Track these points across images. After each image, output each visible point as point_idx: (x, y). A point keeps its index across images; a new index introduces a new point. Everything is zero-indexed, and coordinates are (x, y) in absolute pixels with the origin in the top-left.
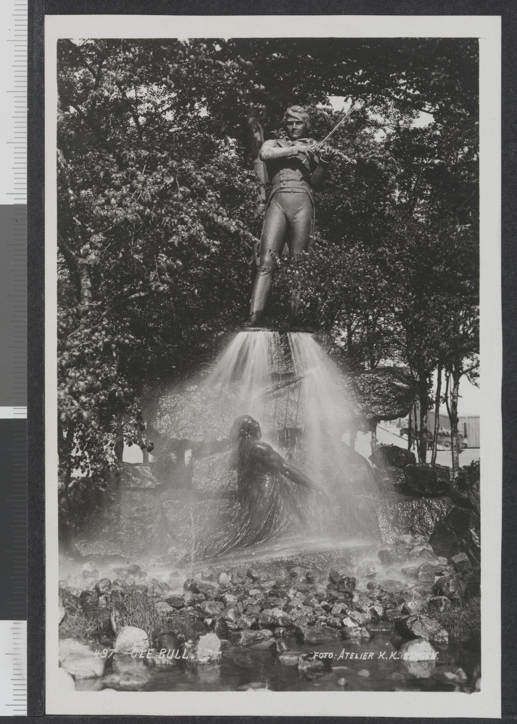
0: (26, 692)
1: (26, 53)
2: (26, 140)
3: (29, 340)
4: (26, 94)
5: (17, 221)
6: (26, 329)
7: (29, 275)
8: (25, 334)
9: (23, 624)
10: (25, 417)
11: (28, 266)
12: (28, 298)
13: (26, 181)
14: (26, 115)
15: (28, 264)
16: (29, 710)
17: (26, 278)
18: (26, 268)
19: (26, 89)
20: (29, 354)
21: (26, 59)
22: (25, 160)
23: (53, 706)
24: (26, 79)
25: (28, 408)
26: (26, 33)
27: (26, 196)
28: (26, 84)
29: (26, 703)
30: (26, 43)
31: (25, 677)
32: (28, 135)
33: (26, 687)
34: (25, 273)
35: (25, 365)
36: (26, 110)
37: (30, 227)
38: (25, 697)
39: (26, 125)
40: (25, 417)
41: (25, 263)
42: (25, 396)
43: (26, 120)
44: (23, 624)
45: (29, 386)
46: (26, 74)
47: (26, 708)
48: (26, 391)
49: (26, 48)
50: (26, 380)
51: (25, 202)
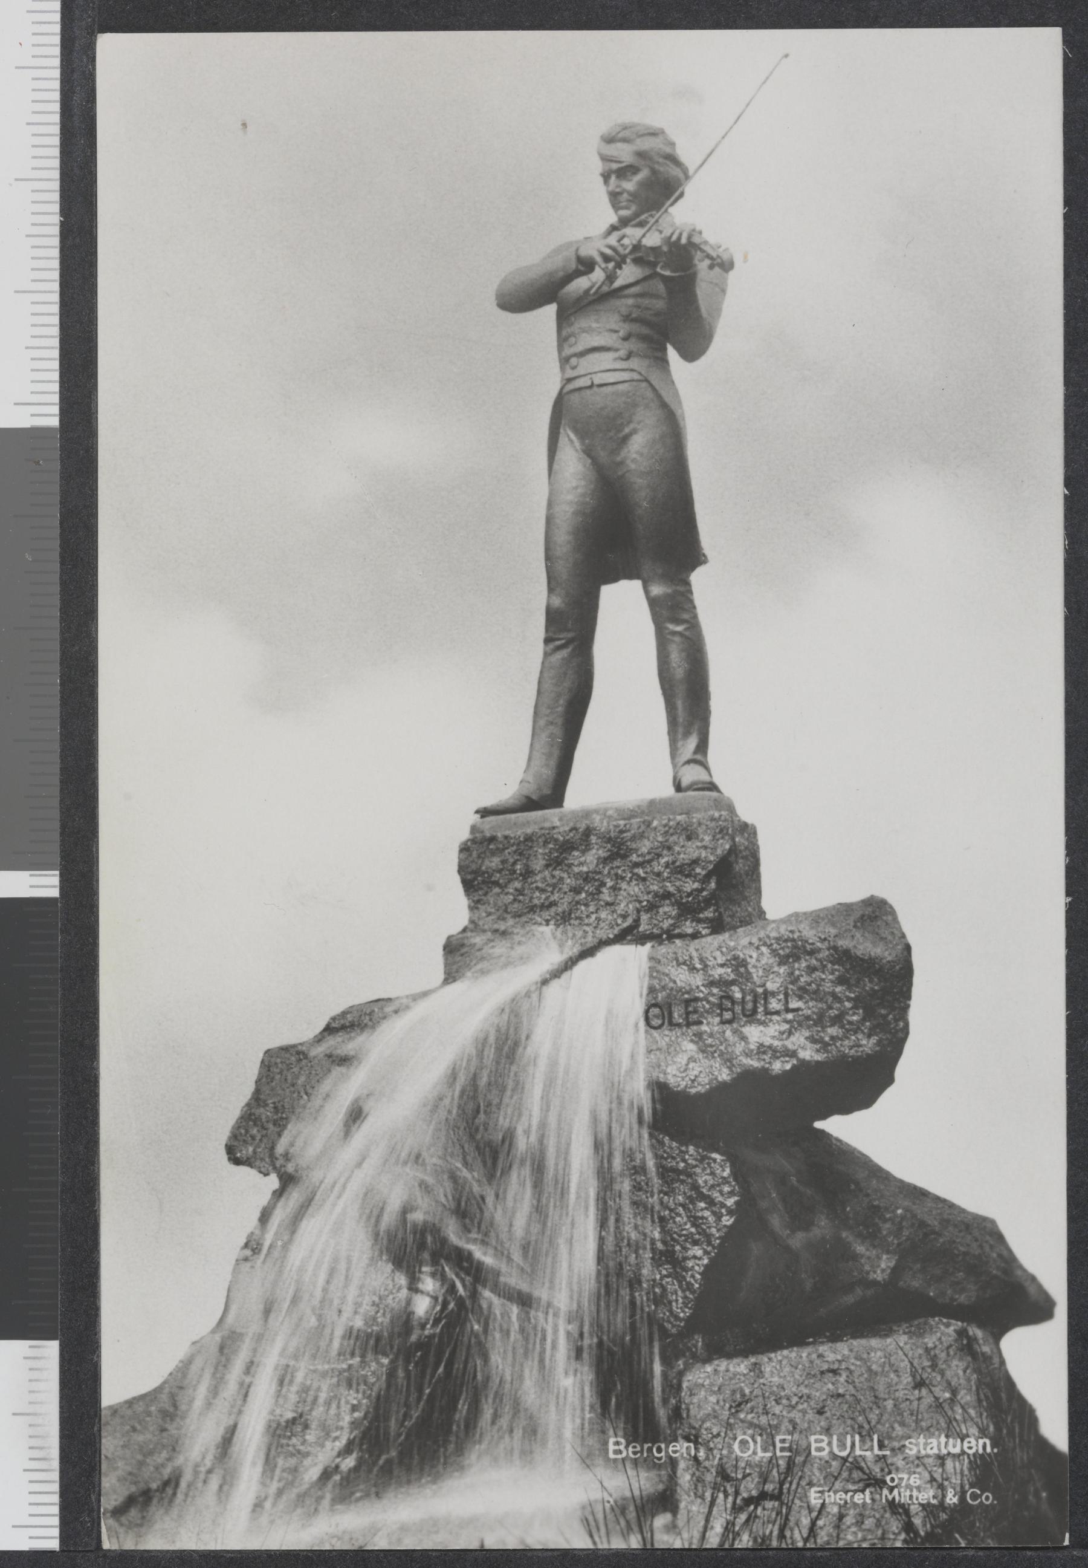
0: (56, 1498)
1: (57, 96)
2: (56, 286)
3: (63, 724)
4: (56, 185)
5: (38, 463)
6: (57, 702)
7: (63, 584)
8: (57, 712)
9: (51, 1349)
10: (55, 893)
11: (62, 563)
12: (62, 633)
13: (56, 376)
14: (56, 230)
15: (62, 557)
16: (64, 1538)
17: (57, 589)
18: (57, 567)
19: (56, 174)
20: (63, 757)
21: (57, 107)
22: (56, 331)
23: (112, 1539)
24: (57, 152)
25: (61, 875)
26: (57, 51)
27: (56, 410)
28: (57, 163)
29: (56, 1521)
30: (57, 73)
31: (56, 1464)
32: (61, 276)
33: (56, 1487)
34: (56, 578)
35: (56, 780)
36: (56, 219)
37: (66, 477)
38: (56, 1510)
39: (56, 253)
40: (55, 893)
41: (56, 556)
42: (56, 848)
43: (56, 241)
44: (51, 1349)
45: (63, 827)
46: (57, 141)
47: (56, 1532)
48: (56, 836)
49: (57, 85)
50: (56, 814)
51: (55, 422)
